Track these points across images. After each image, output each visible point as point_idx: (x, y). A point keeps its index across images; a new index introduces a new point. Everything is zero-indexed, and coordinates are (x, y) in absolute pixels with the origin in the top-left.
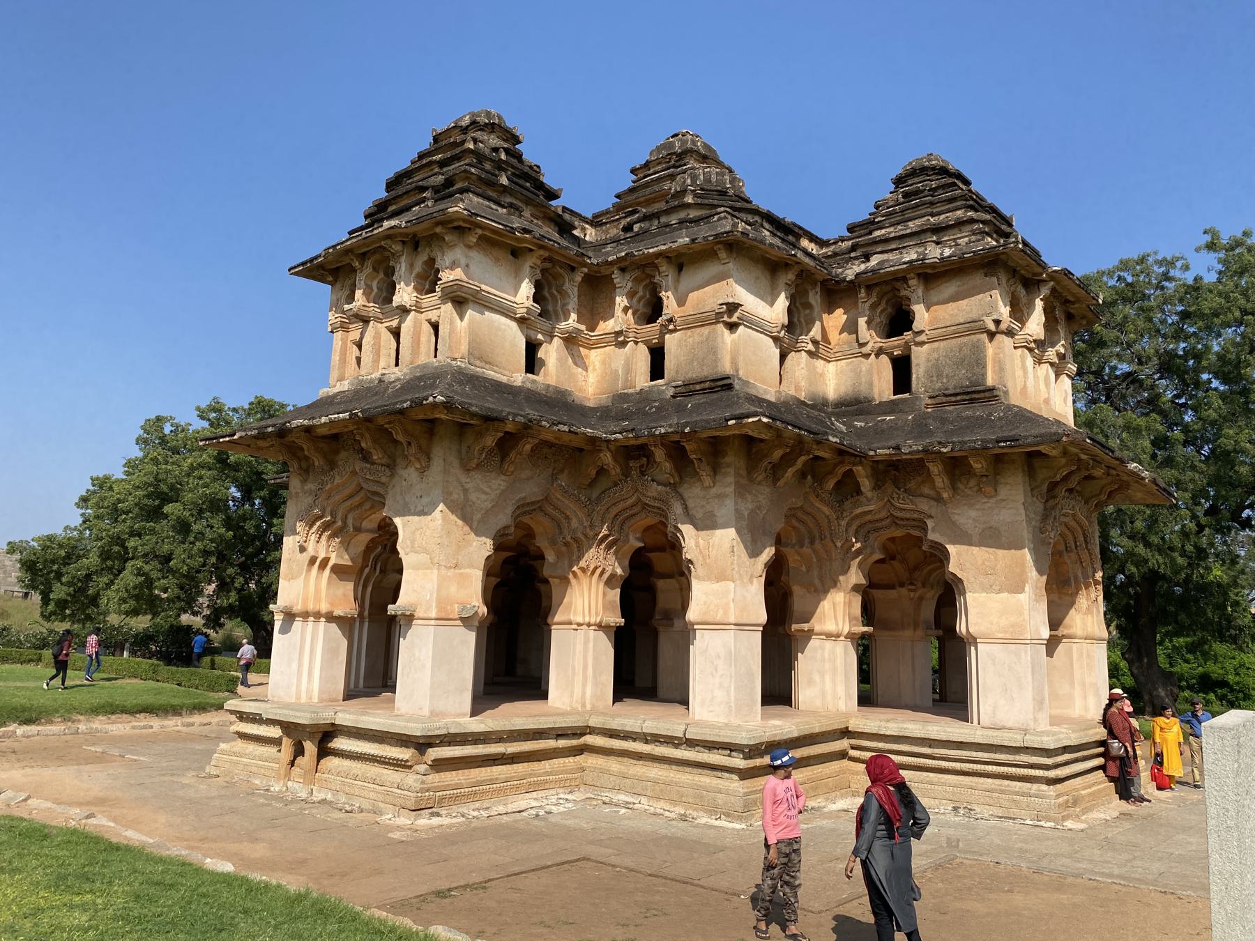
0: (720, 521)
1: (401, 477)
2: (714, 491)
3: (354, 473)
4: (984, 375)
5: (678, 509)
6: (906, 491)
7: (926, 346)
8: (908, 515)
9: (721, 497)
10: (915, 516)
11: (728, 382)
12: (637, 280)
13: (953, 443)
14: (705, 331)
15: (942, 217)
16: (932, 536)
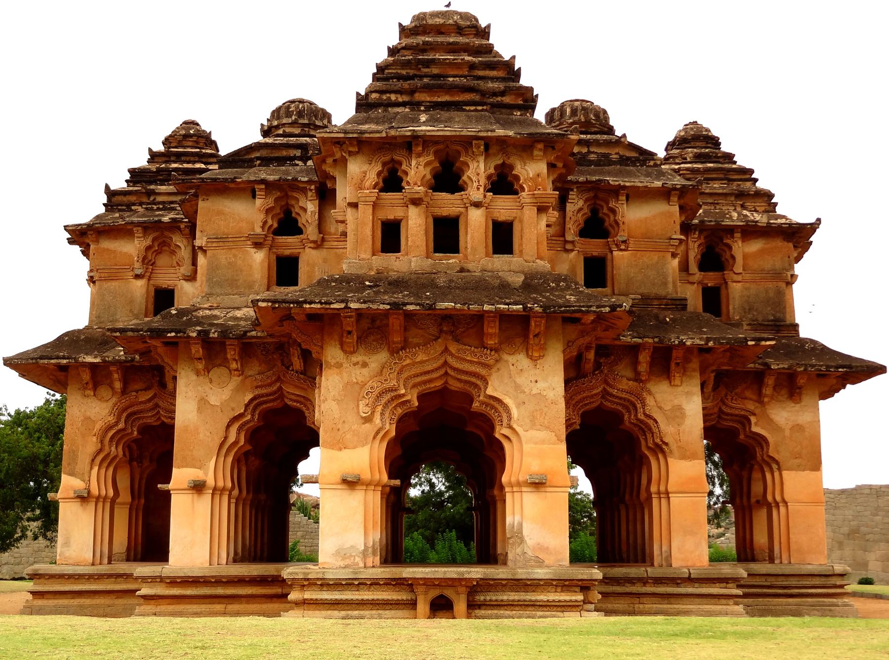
0: (688, 413)
1: (507, 361)
2: (680, 389)
3: (446, 350)
4: (784, 313)
5: (650, 401)
6: (736, 394)
7: (739, 285)
8: (737, 412)
9: (688, 394)
10: (742, 413)
11: (683, 302)
12: (585, 201)
13: (806, 365)
14: (655, 257)
15: (735, 183)
16: (755, 429)
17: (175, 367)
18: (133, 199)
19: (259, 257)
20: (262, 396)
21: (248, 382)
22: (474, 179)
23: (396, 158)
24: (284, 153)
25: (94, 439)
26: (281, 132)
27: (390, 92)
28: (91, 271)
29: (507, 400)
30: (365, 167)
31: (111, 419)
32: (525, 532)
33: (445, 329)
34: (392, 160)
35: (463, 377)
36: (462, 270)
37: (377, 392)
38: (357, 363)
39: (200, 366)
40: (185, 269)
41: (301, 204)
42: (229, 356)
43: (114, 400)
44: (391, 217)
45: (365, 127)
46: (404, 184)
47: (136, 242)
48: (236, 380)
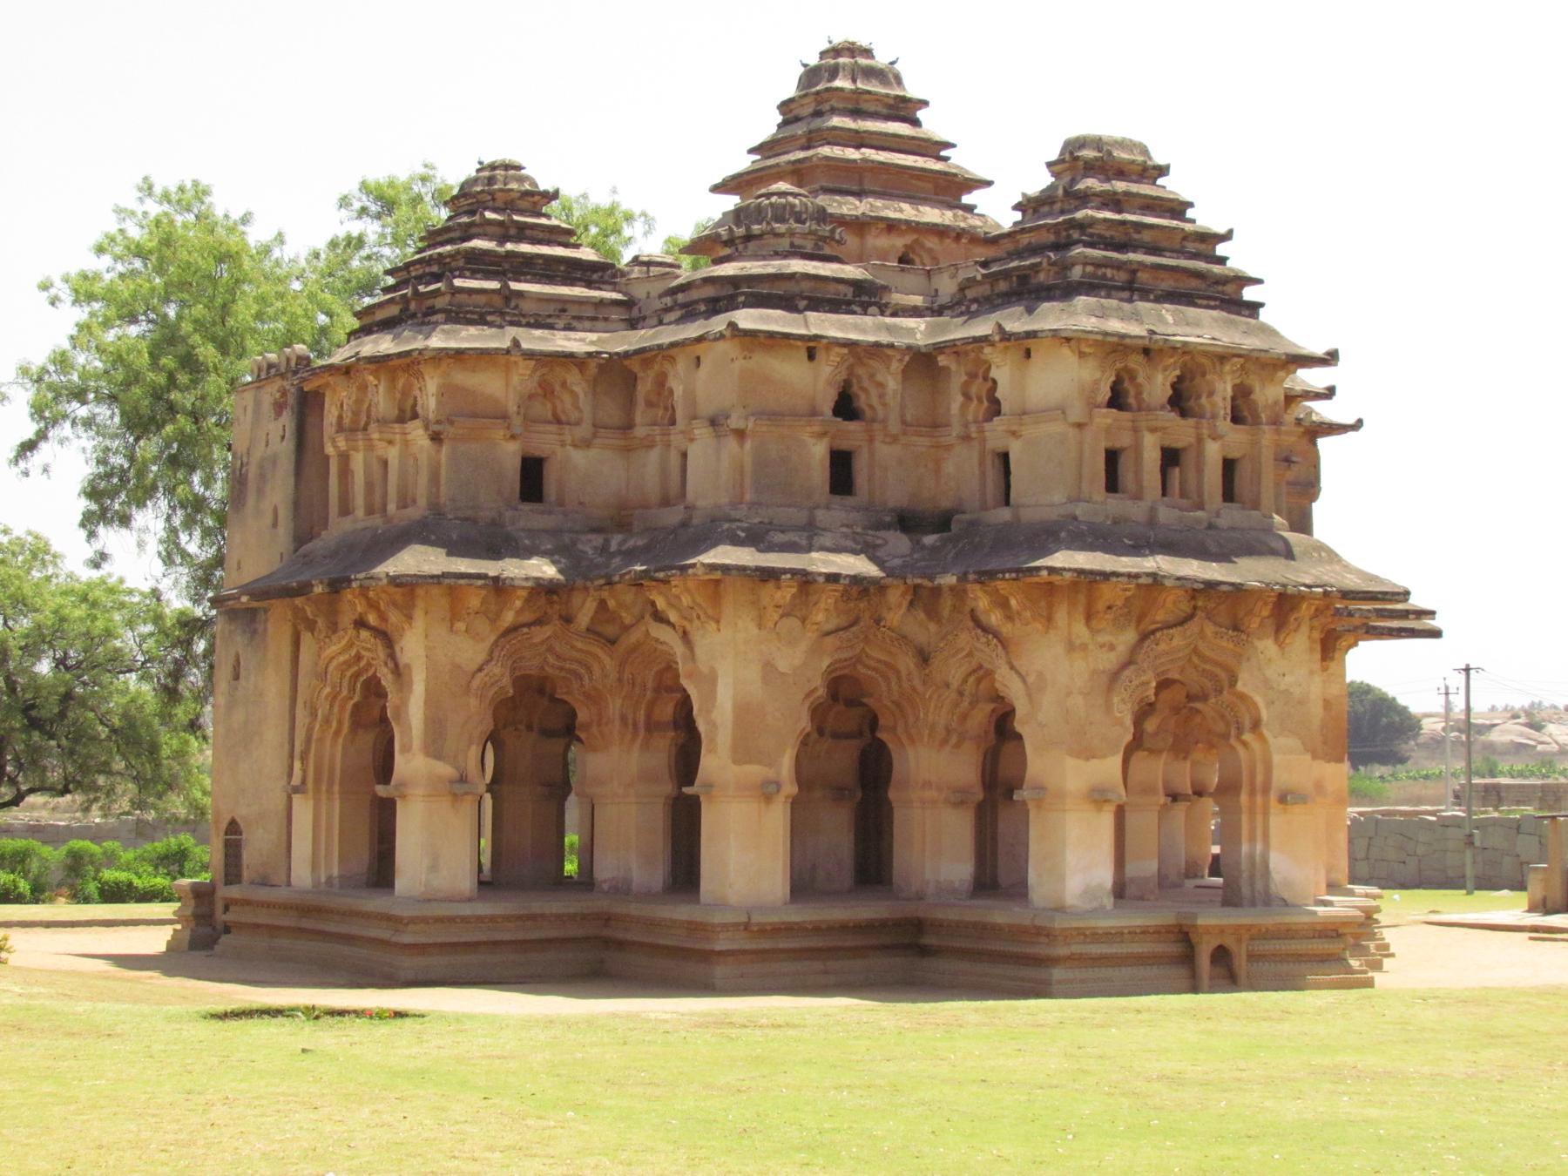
17: (710, 611)
18: (482, 299)
19: (819, 451)
20: (840, 661)
21: (829, 639)
22: (1221, 404)
23: (1132, 365)
24: (831, 291)
25: (473, 702)
27: (1106, 266)
28: (438, 422)
29: (1259, 699)
30: (1098, 375)
31: (497, 670)
32: (1272, 866)
33: (1200, 603)
34: (1127, 370)
35: (1208, 667)
36: (1211, 526)
37: (1136, 682)
38: (1102, 646)
39: (776, 617)
40: (584, 431)
41: (879, 378)
42: (822, 605)
43: (493, 638)
44: (1118, 445)
45: (1115, 325)
46: (1132, 400)
47: (515, 379)
48: (811, 635)
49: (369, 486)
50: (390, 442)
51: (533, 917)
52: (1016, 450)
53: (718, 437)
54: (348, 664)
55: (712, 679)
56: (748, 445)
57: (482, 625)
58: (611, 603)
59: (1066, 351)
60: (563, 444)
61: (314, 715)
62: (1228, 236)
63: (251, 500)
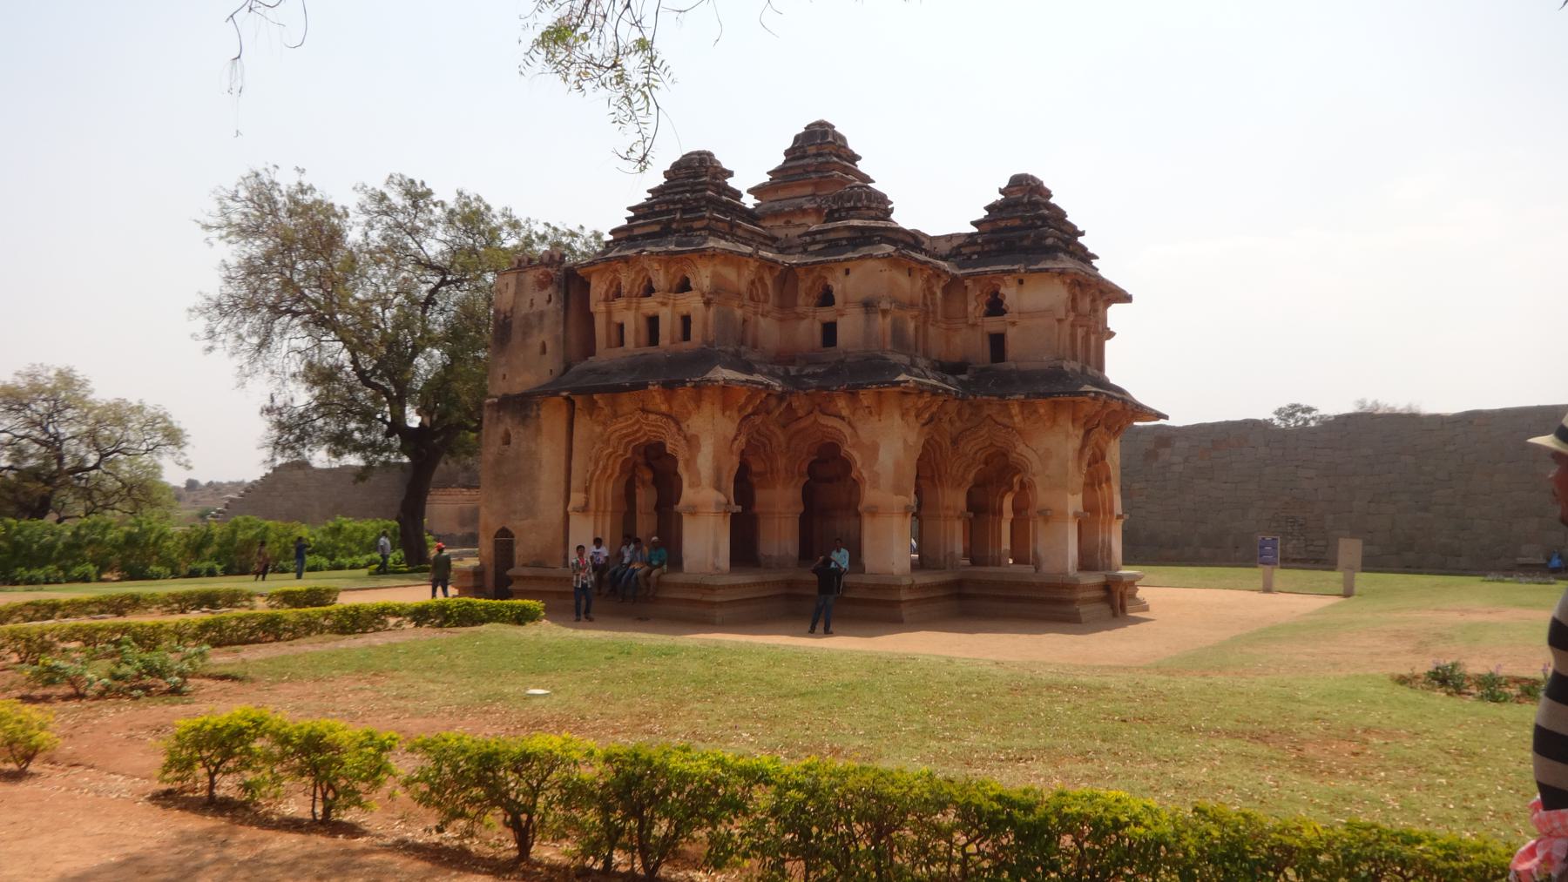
21: (926, 429)
26: (873, 213)
49: (637, 331)
50: (664, 304)
51: (763, 583)
52: (1011, 333)
53: (867, 313)
54: (626, 436)
55: (875, 448)
56: (889, 319)
57: (735, 414)
58: (795, 404)
59: (1057, 281)
60: (756, 314)
61: (597, 464)
62: (1082, 234)
63: (516, 338)
